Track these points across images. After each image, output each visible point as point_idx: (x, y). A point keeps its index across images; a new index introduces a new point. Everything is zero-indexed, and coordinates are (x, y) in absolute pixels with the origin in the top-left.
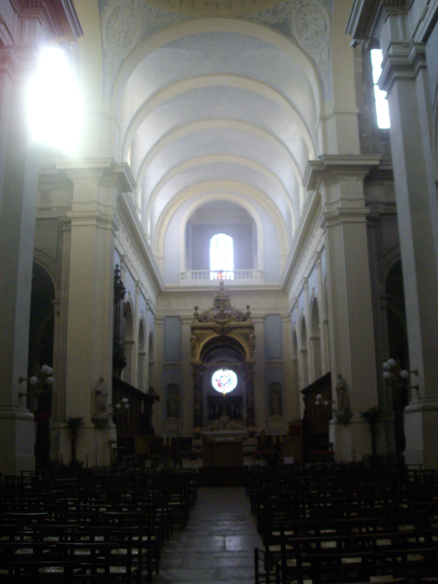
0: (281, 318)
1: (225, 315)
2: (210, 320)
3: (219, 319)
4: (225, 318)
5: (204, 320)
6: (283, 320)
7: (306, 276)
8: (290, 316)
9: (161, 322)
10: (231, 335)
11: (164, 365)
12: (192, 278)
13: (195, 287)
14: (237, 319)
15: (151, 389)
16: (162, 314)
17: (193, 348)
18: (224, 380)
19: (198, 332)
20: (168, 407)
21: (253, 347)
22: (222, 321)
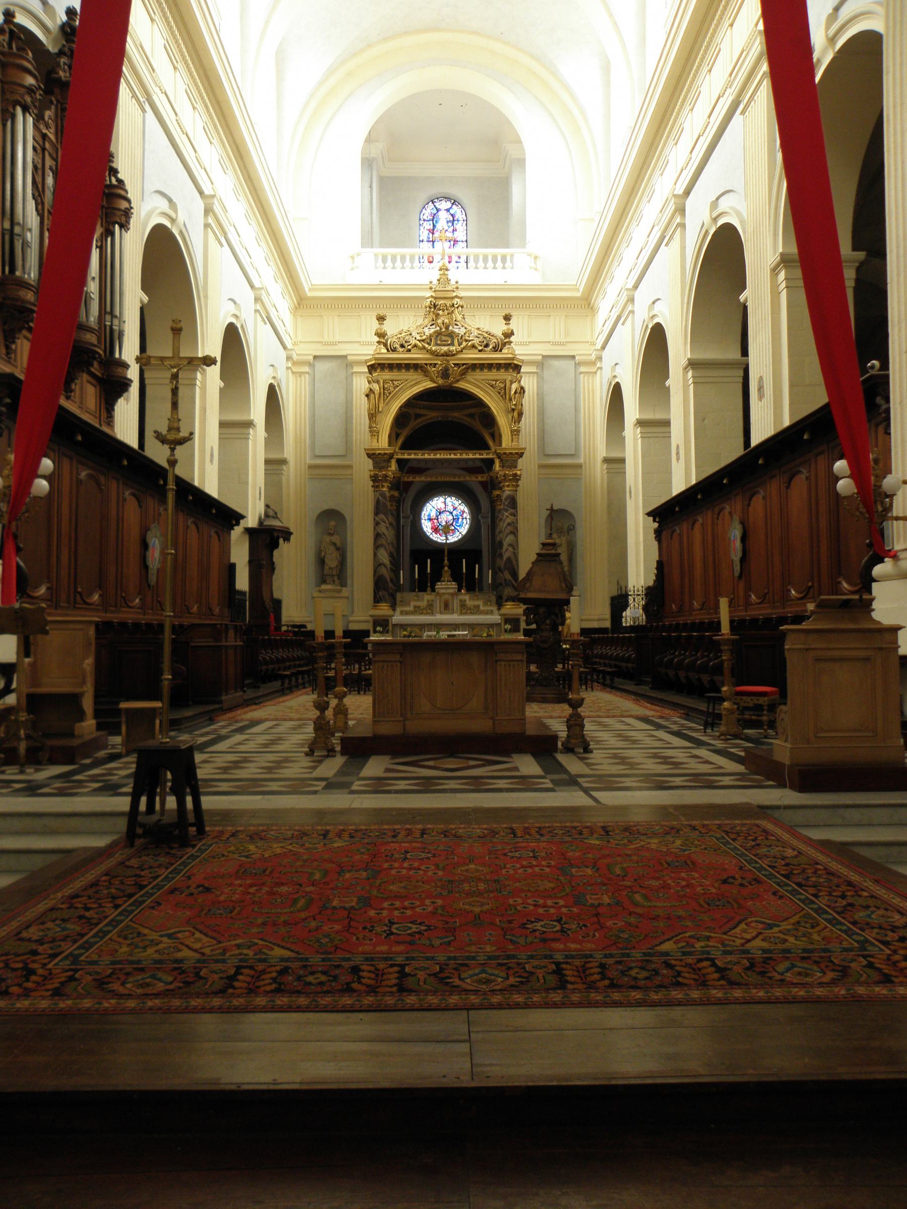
0: (578, 365)
1: (452, 335)
2: (415, 346)
3: (437, 344)
4: (452, 344)
5: (401, 350)
6: (582, 369)
7: (680, 190)
8: (600, 358)
9: (306, 369)
10: (463, 385)
11: (311, 467)
12: (376, 268)
13: (380, 287)
14: (480, 348)
15: (270, 512)
16: (307, 351)
17: (373, 416)
18: (445, 518)
19: (387, 375)
20: (321, 562)
21: (517, 414)
22: (445, 348)
